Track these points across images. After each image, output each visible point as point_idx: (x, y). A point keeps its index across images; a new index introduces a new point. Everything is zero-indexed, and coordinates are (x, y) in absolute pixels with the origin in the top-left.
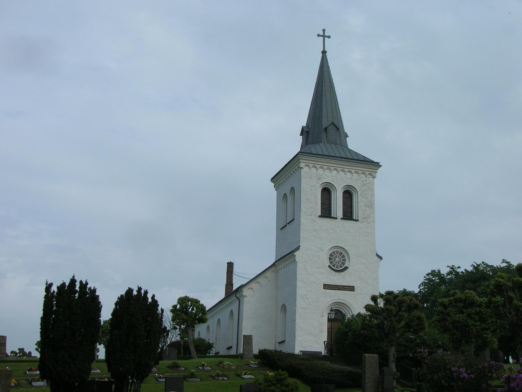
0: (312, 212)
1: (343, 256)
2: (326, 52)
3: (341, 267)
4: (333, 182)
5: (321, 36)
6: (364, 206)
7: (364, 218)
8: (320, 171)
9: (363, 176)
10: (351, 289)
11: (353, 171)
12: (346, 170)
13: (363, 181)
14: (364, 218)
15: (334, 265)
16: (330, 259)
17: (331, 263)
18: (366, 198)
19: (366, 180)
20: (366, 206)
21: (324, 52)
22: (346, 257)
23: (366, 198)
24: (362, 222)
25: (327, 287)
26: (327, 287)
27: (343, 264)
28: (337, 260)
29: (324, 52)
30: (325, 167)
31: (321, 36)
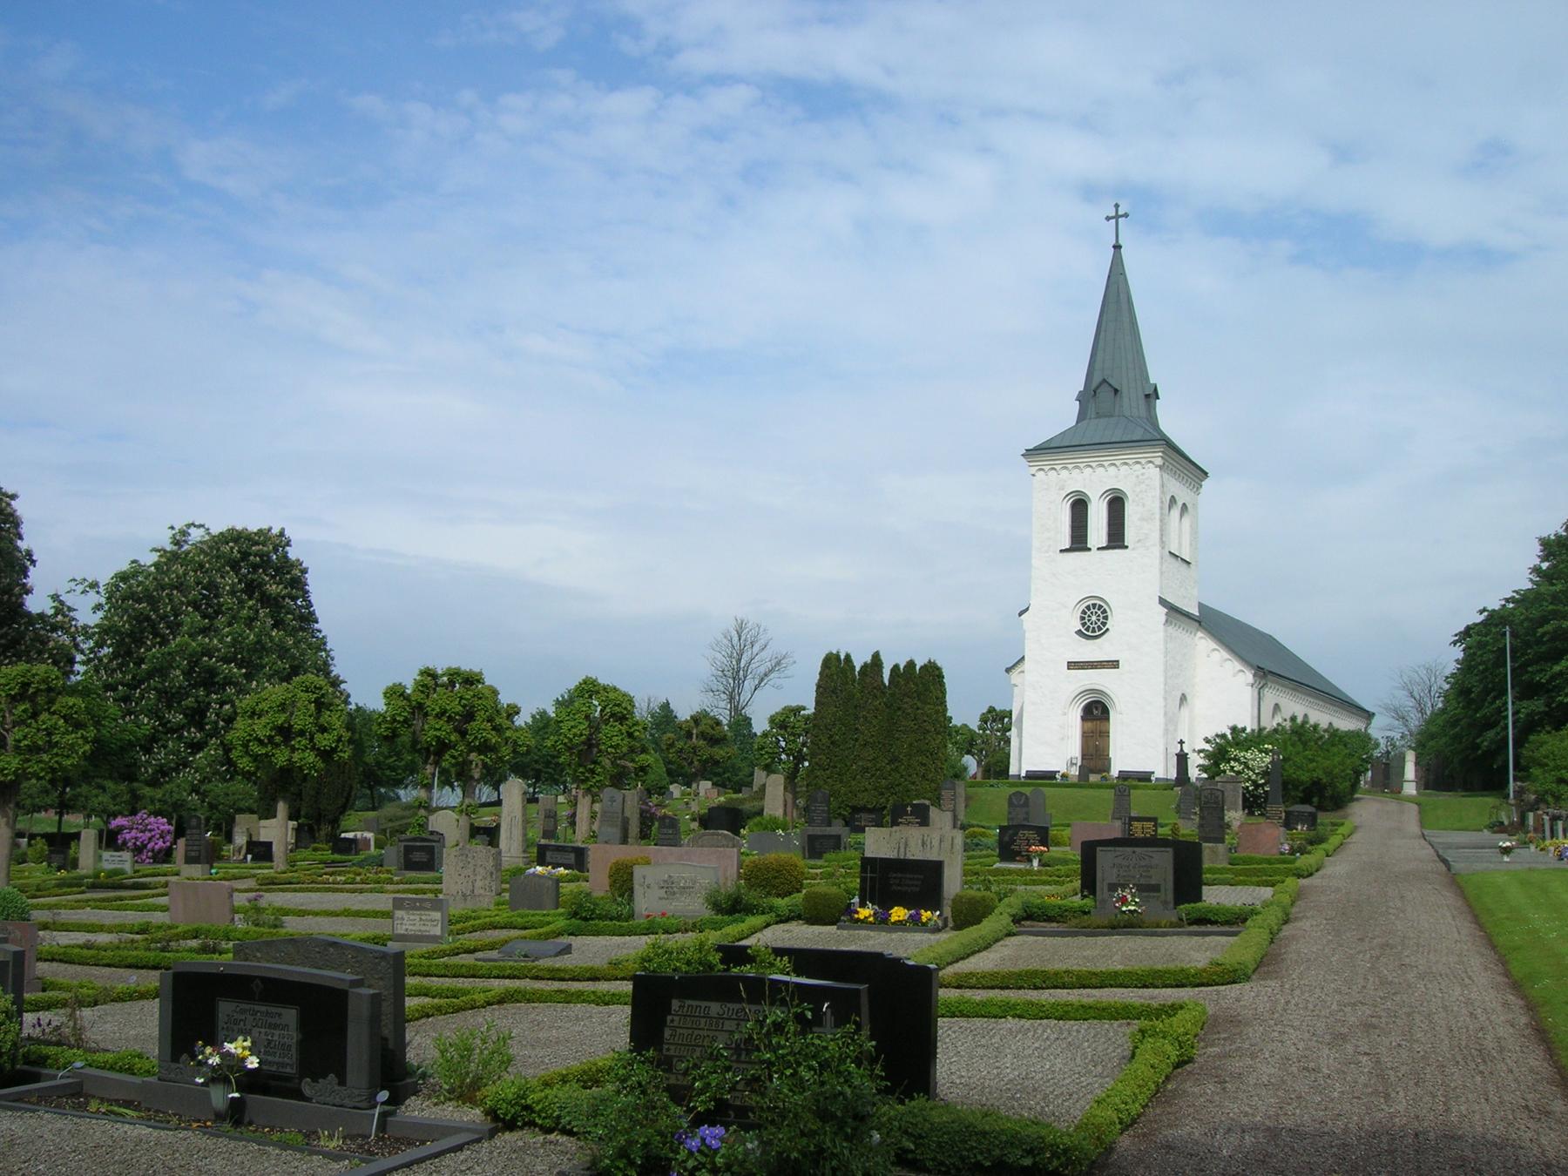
0: (1050, 546)
1: (1105, 611)
2: (1120, 247)
3: (1100, 629)
4: (1085, 487)
5: (1122, 216)
6: (1139, 519)
7: (1139, 541)
8: (1064, 473)
9: (1138, 466)
10: (1114, 664)
11: (1118, 463)
12: (1106, 464)
13: (1137, 477)
14: (1139, 541)
15: (1087, 630)
16: (1082, 618)
17: (1084, 625)
18: (1144, 505)
19: (1143, 474)
20: (1142, 519)
21: (1117, 247)
22: (1109, 613)
23: (1144, 505)
24: (1133, 549)
25: (1073, 665)
26: (1073, 665)
27: (1104, 624)
28: (1094, 618)
29: (1117, 247)
30: (1070, 466)
31: (1122, 216)
